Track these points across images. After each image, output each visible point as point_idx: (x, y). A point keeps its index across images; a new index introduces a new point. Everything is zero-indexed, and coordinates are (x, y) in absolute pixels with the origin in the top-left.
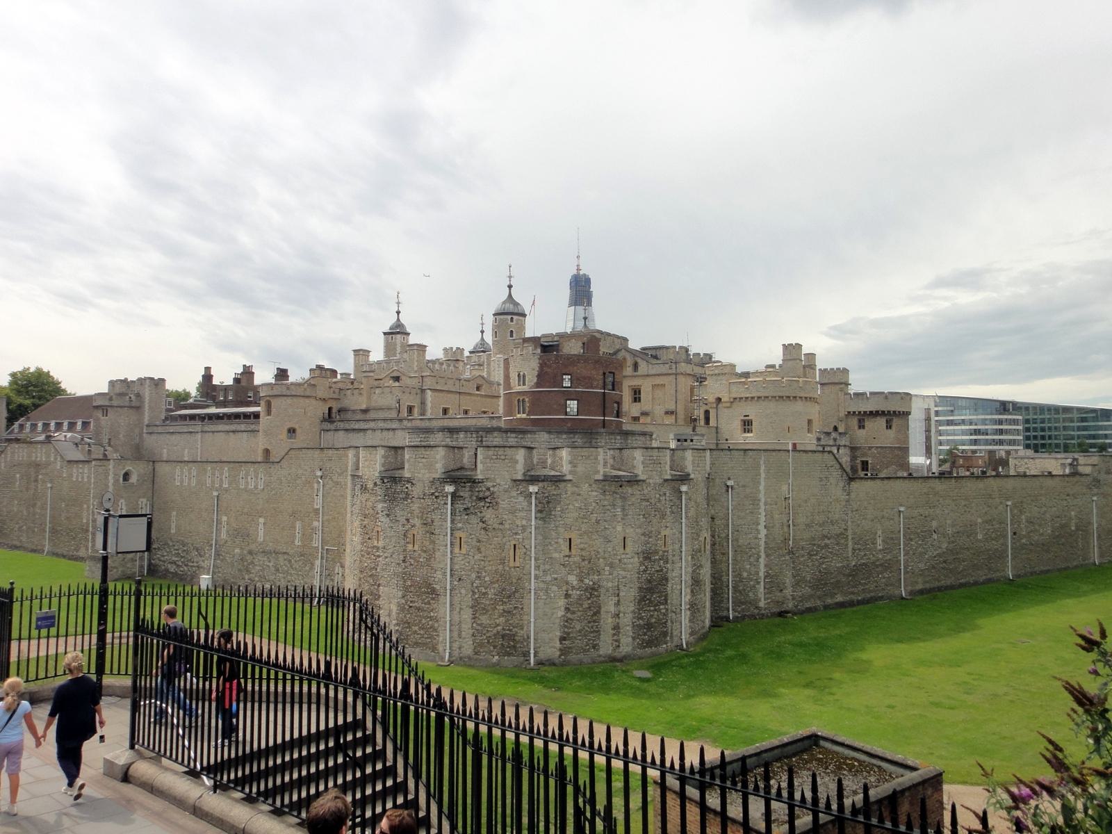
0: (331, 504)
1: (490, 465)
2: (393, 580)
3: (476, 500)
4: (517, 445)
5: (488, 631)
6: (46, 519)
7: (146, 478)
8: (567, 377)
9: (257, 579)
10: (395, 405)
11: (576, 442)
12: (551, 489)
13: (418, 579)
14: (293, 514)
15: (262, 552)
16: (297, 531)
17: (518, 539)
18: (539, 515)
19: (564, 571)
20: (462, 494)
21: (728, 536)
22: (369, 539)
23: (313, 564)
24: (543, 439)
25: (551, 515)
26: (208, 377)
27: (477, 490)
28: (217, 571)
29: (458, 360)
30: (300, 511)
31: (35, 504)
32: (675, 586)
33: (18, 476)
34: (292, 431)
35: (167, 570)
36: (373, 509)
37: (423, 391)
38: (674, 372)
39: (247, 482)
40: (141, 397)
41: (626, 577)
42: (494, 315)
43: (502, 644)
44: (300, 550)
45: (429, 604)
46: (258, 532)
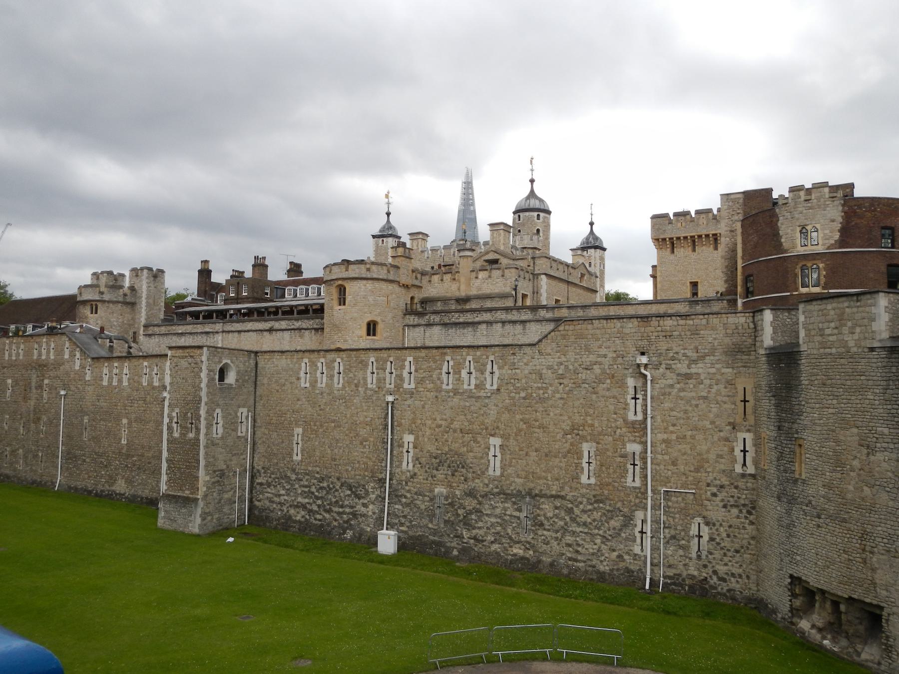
0: (674, 413)
6: (58, 440)
9: (490, 538)
14: (574, 428)
15: (499, 494)
16: (586, 459)
26: (205, 273)
29: (535, 248)
30: (592, 425)
31: (39, 419)
33: (9, 381)
34: (371, 329)
35: (289, 518)
37: (536, 276)
40: (136, 292)
42: (514, 213)
44: (594, 493)
46: (489, 461)
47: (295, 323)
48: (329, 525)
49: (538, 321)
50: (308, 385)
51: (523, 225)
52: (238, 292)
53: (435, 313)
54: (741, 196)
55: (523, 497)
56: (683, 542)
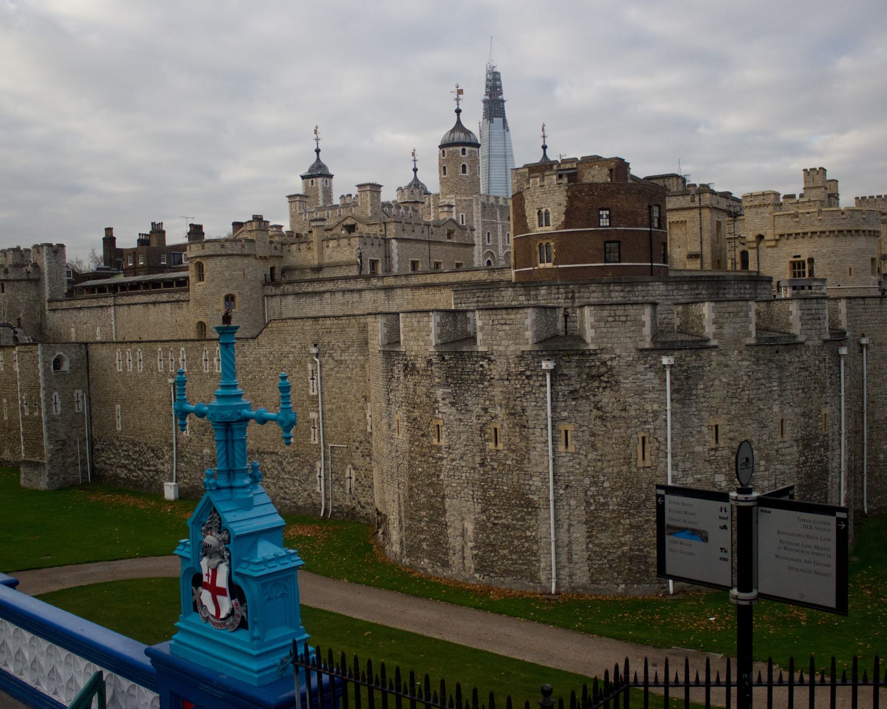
0: (334, 390)
1: (605, 330)
2: (466, 490)
3: (587, 379)
4: (624, 300)
5: (609, 552)
7: (79, 365)
8: (604, 213)
10: (354, 257)
11: (699, 294)
12: (690, 359)
13: (505, 488)
17: (649, 429)
18: (675, 396)
19: (709, 469)
20: (566, 371)
21: (863, 409)
22: (423, 435)
23: (313, 467)
24: (658, 292)
25: (691, 394)
26: (109, 240)
27: (587, 365)
28: (181, 475)
29: (417, 202)
32: (834, 480)
35: (116, 476)
36: (428, 397)
37: (387, 241)
38: (698, 205)
39: (213, 365)
40: (39, 268)
41: (784, 473)
42: (441, 147)
43: (630, 569)
44: (293, 449)
45: (524, 520)
47: (174, 295)
48: (141, 480)
49: (371, 289)
50: (121, 370)
51: (448, 161)
52: (135, 262)
53: (289, 283)
54: (527, 170)
55: (254, 454)
56: (342, 482)
